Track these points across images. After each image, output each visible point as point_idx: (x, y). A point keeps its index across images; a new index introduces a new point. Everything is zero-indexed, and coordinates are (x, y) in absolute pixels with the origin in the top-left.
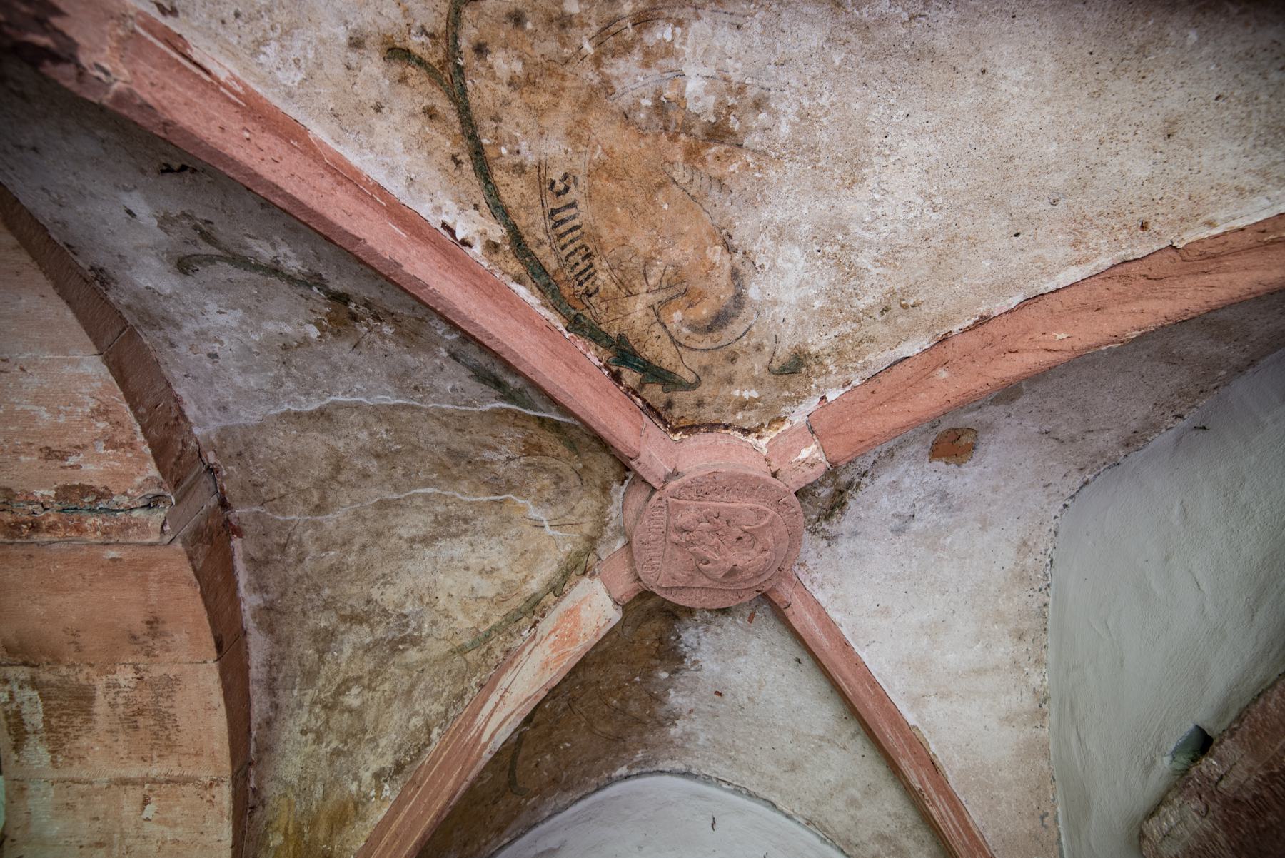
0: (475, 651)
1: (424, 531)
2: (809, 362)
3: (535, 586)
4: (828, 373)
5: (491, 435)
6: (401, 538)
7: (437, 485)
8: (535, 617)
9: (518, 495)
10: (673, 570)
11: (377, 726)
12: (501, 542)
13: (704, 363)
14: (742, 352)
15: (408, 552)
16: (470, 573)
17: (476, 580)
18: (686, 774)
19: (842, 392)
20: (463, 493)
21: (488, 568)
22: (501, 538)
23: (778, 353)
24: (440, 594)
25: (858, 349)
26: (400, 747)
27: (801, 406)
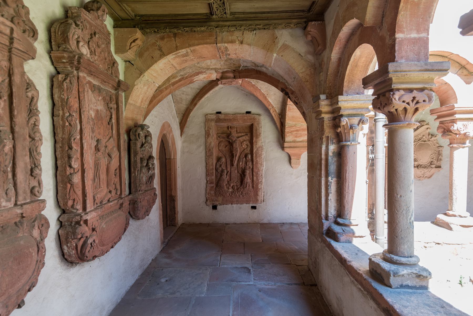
3: (211, 67)
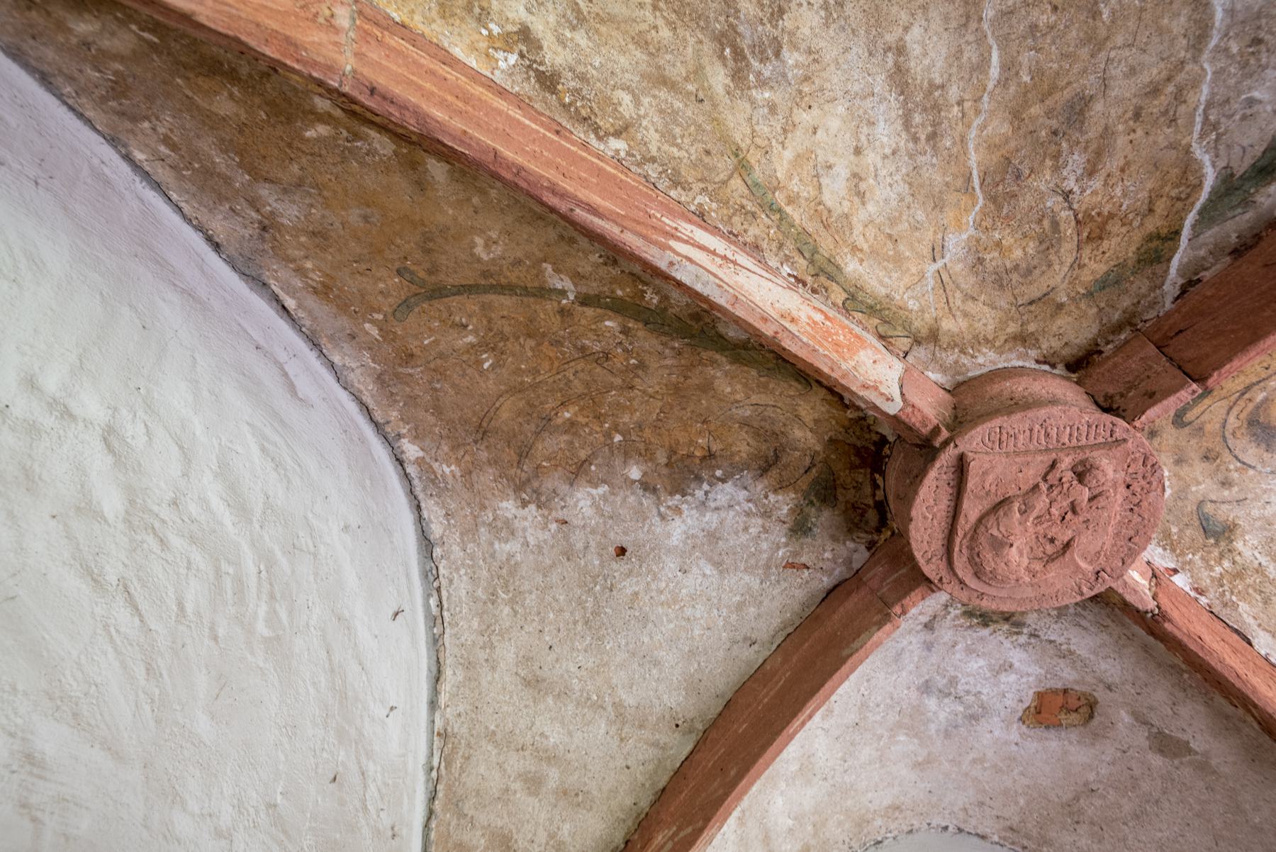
0: (747, 192)
1: (916, 67)
2: (1223, 544)
3: (852, 267)
4: (1211, 569)
5: (1128, 164)
6: (906, 29)
7: (1003, 83)
8: (809, 279)
9: (984, 214)
10: (999, 469)
11: (602, 21)
12: (902, 200)
13: (1208, 427)
14: (1218, 466)
15: (880, 45)
16: (852, 157)
17: (842, 171)
18: (427, 543)
19: (1187, 589)
20: (983, 127)
21: (863, 186)
22: (909, 199)
23: (1224, 507)
24: (815, 112)
25: (1251, 591)
26: (583, 78)
27: (1160, 550)
